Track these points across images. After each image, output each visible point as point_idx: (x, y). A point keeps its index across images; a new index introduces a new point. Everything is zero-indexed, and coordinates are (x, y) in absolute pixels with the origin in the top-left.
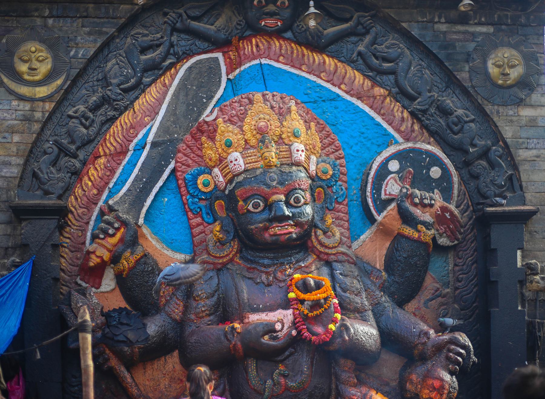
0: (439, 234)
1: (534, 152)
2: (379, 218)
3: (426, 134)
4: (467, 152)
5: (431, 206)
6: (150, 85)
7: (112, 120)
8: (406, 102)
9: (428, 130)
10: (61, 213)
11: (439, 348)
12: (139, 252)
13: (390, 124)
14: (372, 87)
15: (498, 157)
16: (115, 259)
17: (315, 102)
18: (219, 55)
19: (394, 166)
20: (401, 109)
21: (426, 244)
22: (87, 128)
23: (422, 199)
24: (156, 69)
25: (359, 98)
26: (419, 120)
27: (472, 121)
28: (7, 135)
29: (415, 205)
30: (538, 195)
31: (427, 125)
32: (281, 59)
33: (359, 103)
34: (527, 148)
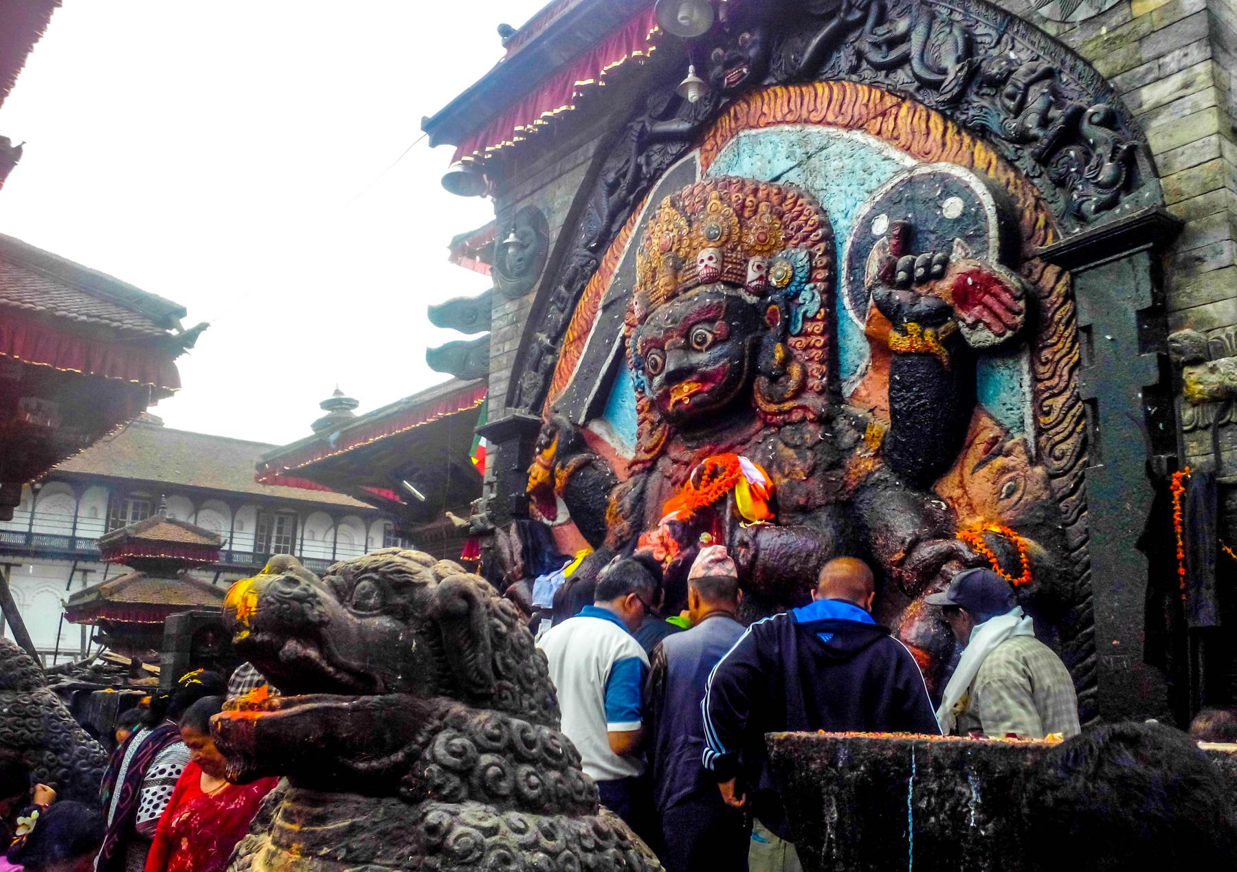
0: (968, 325)
1: (1177, 79)
3: (967, 140)
5: (940, 276)
6: (619, 231)
13: (908, 149)
14: (882, 97)
15: (1099, 124)
16: (552, 476)
17: (799, 165)
18: (696, 154)
19: (881, 226)
20: (924, 114)
21: (926, 354)
22: (562, 311)
25: (860, 127)
28: (500, 346)
29: (905, 285)
30: (1195, 171)
31: (964, 121)
32: (763, 120)
33: (857, 135)
34: (1158, 79)
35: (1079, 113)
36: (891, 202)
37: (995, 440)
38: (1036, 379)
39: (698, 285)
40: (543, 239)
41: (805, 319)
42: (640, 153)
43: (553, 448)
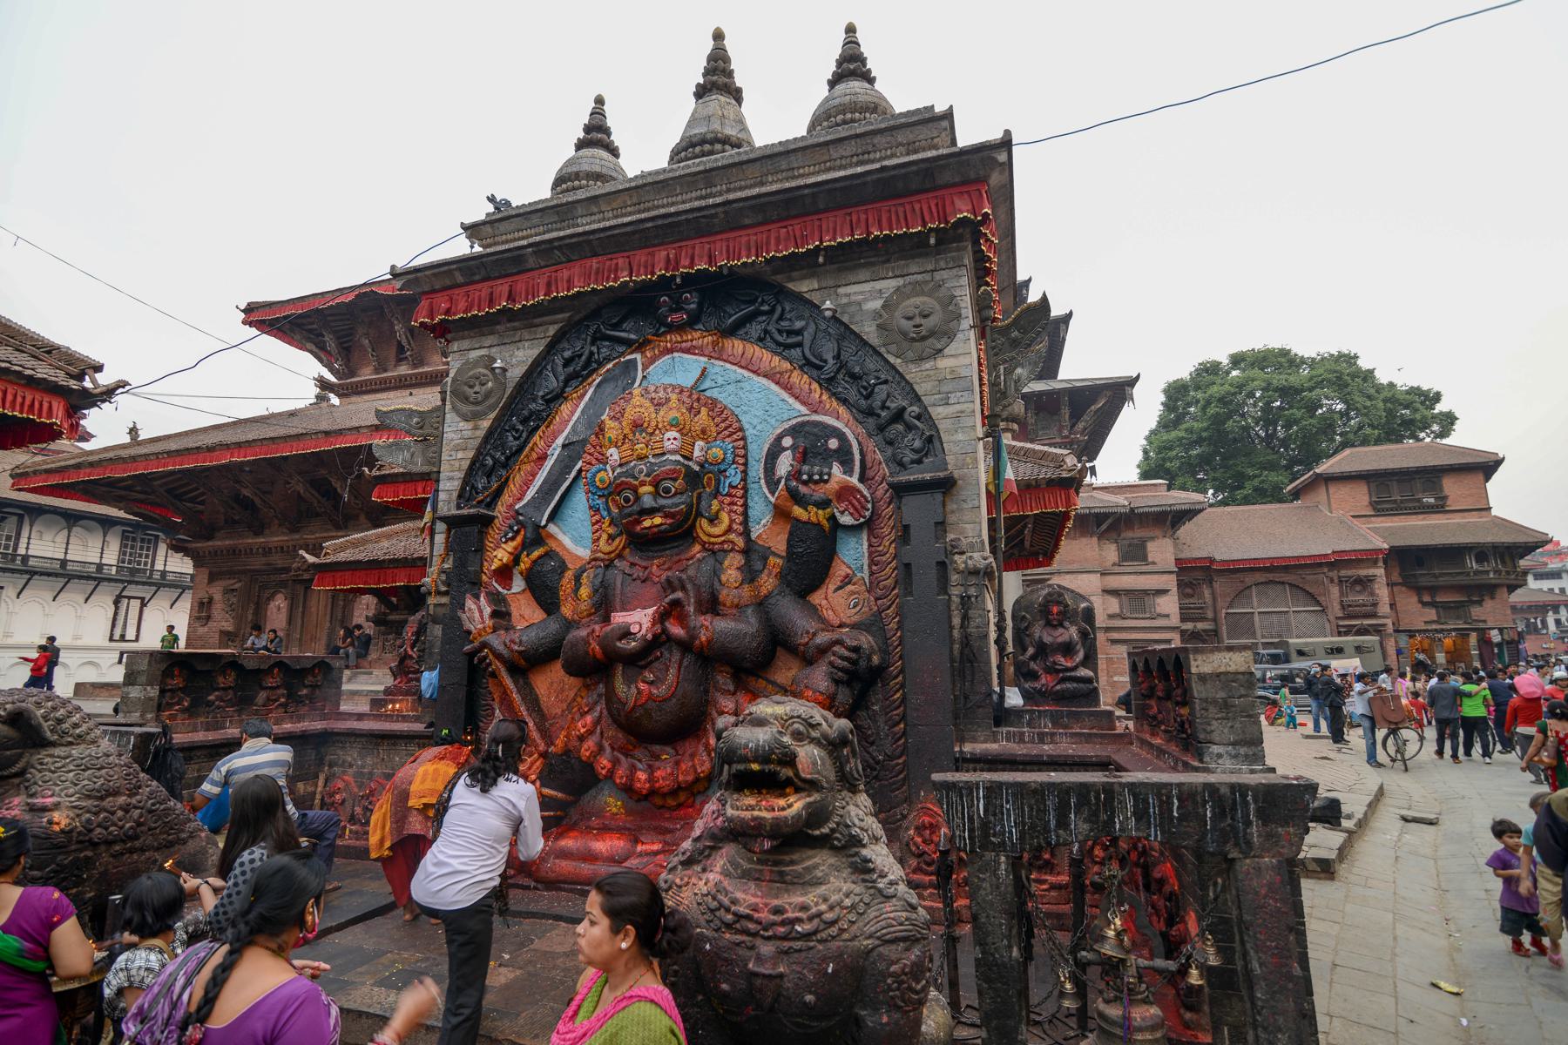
1: (958, 407)
2: (773, 500)
4: (879, 416)
5: (826, 482)
7: (536, 428)
8: (815, 373)
9: (838, 399)
10: (488, 521)
11: (823, 650)
12: (536, 554)
16: (516, 560)
18: (638, 356)
19: (787, 442)
23: (810, 476)
24: (577, 377)
26: (827, 389)
27: (886, 382)
29: (805, 483)
33: (764, 381)
35: (904, 409)
36: (794, 431)
37: (847, 576)
38: (870, 546)
39: (663, 454)
40: (503, 386)
41: (731, 486)
42: (593, 343)
43: (519, 539)
